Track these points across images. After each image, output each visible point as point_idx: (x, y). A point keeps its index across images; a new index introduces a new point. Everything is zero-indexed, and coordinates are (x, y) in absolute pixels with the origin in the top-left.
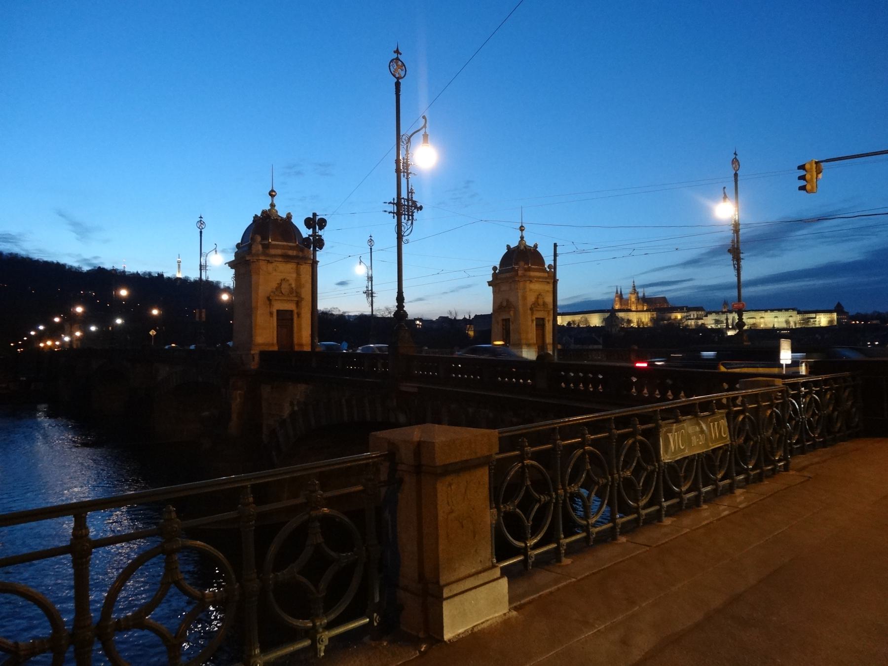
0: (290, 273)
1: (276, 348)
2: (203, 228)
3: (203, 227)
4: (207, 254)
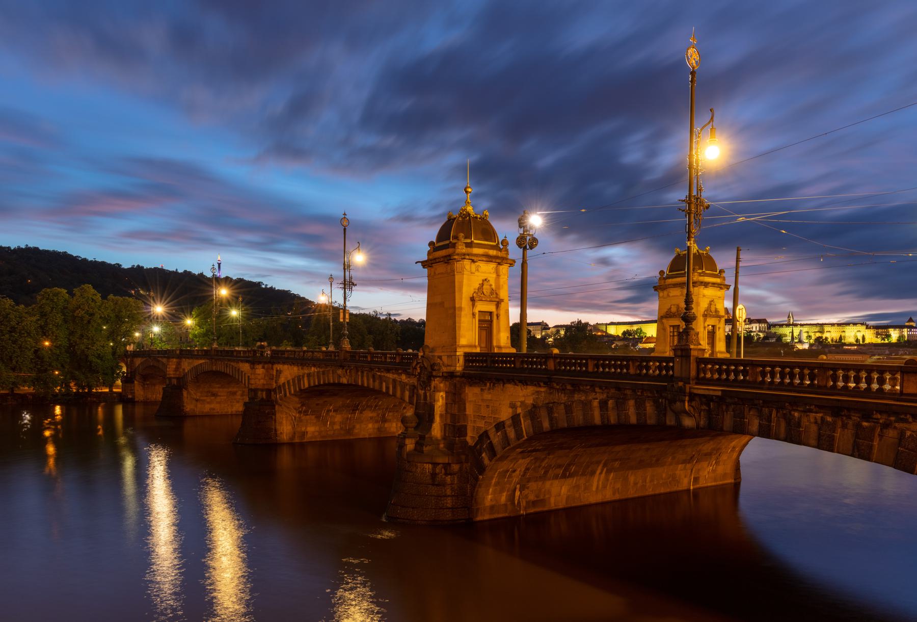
0: (490, 273)
1: (478, 350)
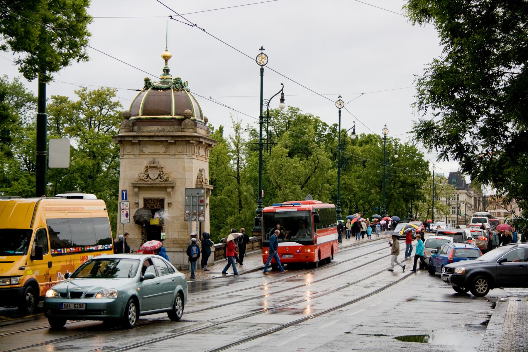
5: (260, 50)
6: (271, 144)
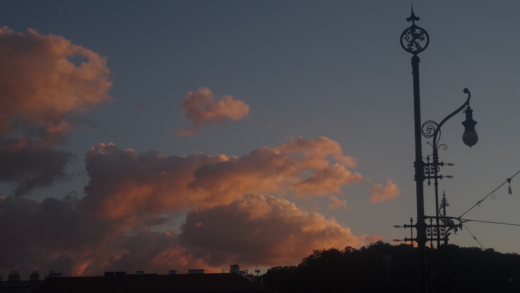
2: (421, 50)
3: (422, 44)
4: (439, 126)
5: (408, 20)
6: (447, 228)
